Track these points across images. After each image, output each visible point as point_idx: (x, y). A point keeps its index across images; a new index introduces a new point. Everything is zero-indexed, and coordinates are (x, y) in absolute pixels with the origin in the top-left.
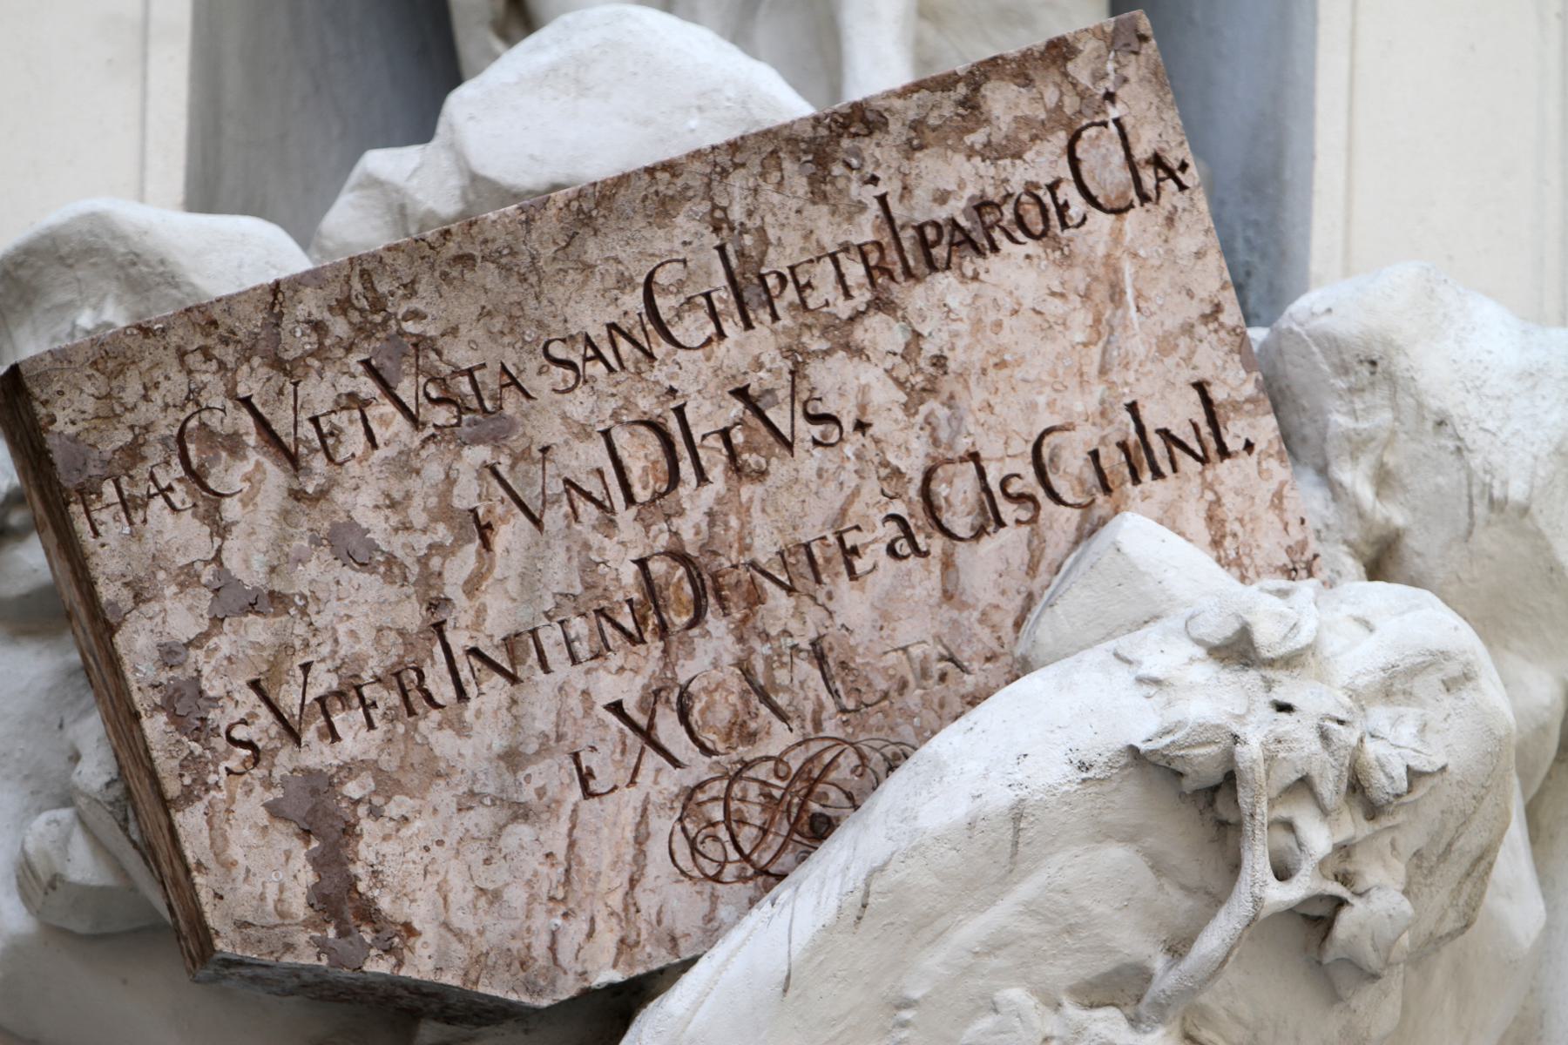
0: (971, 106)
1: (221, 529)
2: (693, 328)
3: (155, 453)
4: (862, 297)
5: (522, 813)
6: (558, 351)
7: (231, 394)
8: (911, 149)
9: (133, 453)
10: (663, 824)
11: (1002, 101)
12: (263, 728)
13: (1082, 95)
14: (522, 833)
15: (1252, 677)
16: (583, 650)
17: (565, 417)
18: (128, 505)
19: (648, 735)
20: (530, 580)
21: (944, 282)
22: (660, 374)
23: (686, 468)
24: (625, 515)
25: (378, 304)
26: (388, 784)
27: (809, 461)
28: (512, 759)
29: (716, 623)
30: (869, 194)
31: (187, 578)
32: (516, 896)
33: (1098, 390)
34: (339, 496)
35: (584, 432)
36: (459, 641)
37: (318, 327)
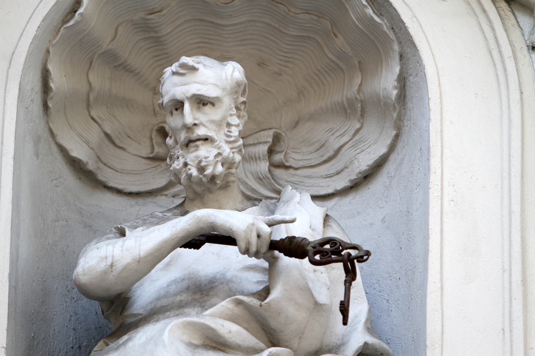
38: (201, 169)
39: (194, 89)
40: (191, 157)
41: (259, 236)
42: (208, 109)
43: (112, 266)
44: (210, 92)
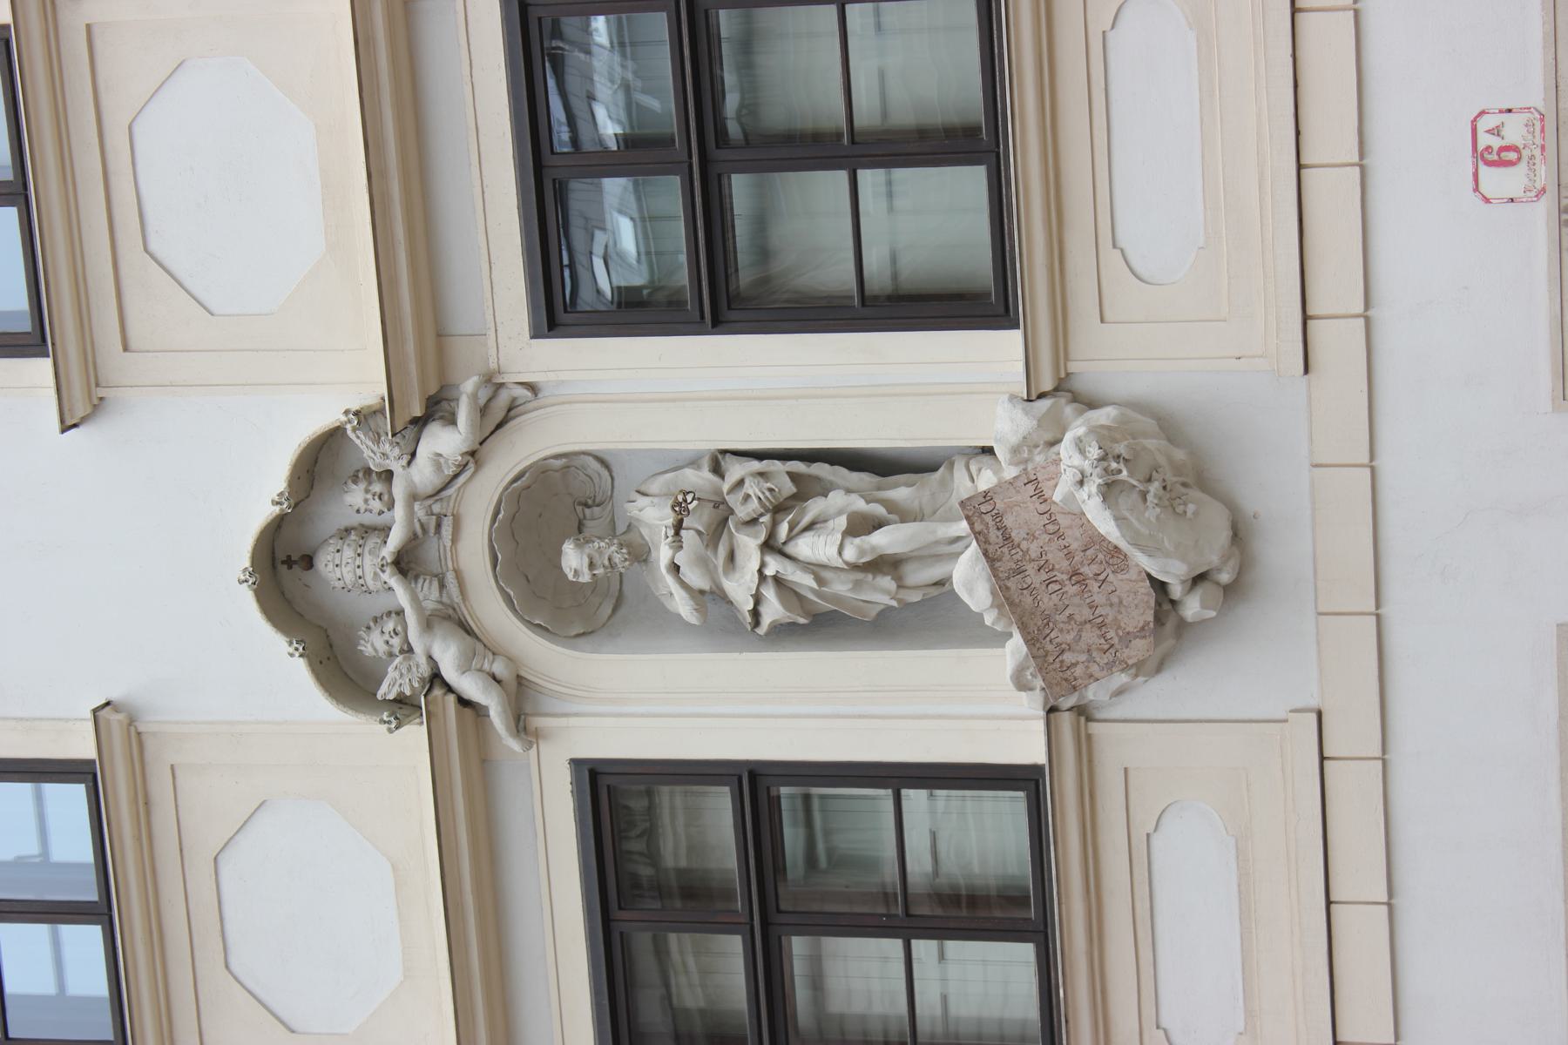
0: (979, 533)
1: (1077, 663)
2: (1028, 580)
3: (1065, 676)
4: (1018, 550)
5: (1121, 602)
6: (1036, 605)
7: (1052, 663)
8: (990, 544)
9: (1066, 680)
10: (1120, 576)
11: (978, 527)
12: (1112, 651)
13: (974, 513)
14: (1125, 603)
15: (1085, 480)
16: (1090, 594)
17: (1048, 602)
18: (1075, 680)
19: (1104, 580)
20: (1079, 606)
21: (1013, 534)
22: (1038, 586)
23: (1054, 579)
24: (1064, 589)
25: (1033, 639)
26: (1119, 627)
27: (1050, 556)
28: (1111, 605)
29: (1082, 570)
30: (999, 550)
31: (1087, 667)
32: (1136, 602)
33: (1029, 504)
34: (1068, 642)
35: (1050, 599)
36: (1092, 617)
37: (1039, 649)
38: (626, 559)
39: (586, 570)
40: (619, 566)
41: (674, 542)
42: (594, 561)
43: (695, 609)
44: (586, 561)
